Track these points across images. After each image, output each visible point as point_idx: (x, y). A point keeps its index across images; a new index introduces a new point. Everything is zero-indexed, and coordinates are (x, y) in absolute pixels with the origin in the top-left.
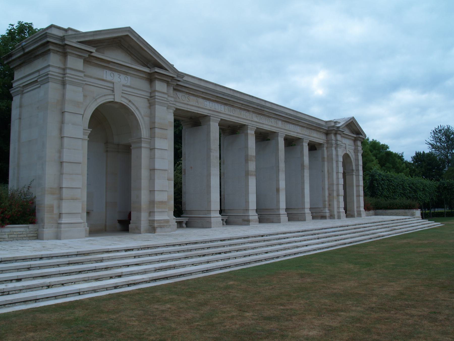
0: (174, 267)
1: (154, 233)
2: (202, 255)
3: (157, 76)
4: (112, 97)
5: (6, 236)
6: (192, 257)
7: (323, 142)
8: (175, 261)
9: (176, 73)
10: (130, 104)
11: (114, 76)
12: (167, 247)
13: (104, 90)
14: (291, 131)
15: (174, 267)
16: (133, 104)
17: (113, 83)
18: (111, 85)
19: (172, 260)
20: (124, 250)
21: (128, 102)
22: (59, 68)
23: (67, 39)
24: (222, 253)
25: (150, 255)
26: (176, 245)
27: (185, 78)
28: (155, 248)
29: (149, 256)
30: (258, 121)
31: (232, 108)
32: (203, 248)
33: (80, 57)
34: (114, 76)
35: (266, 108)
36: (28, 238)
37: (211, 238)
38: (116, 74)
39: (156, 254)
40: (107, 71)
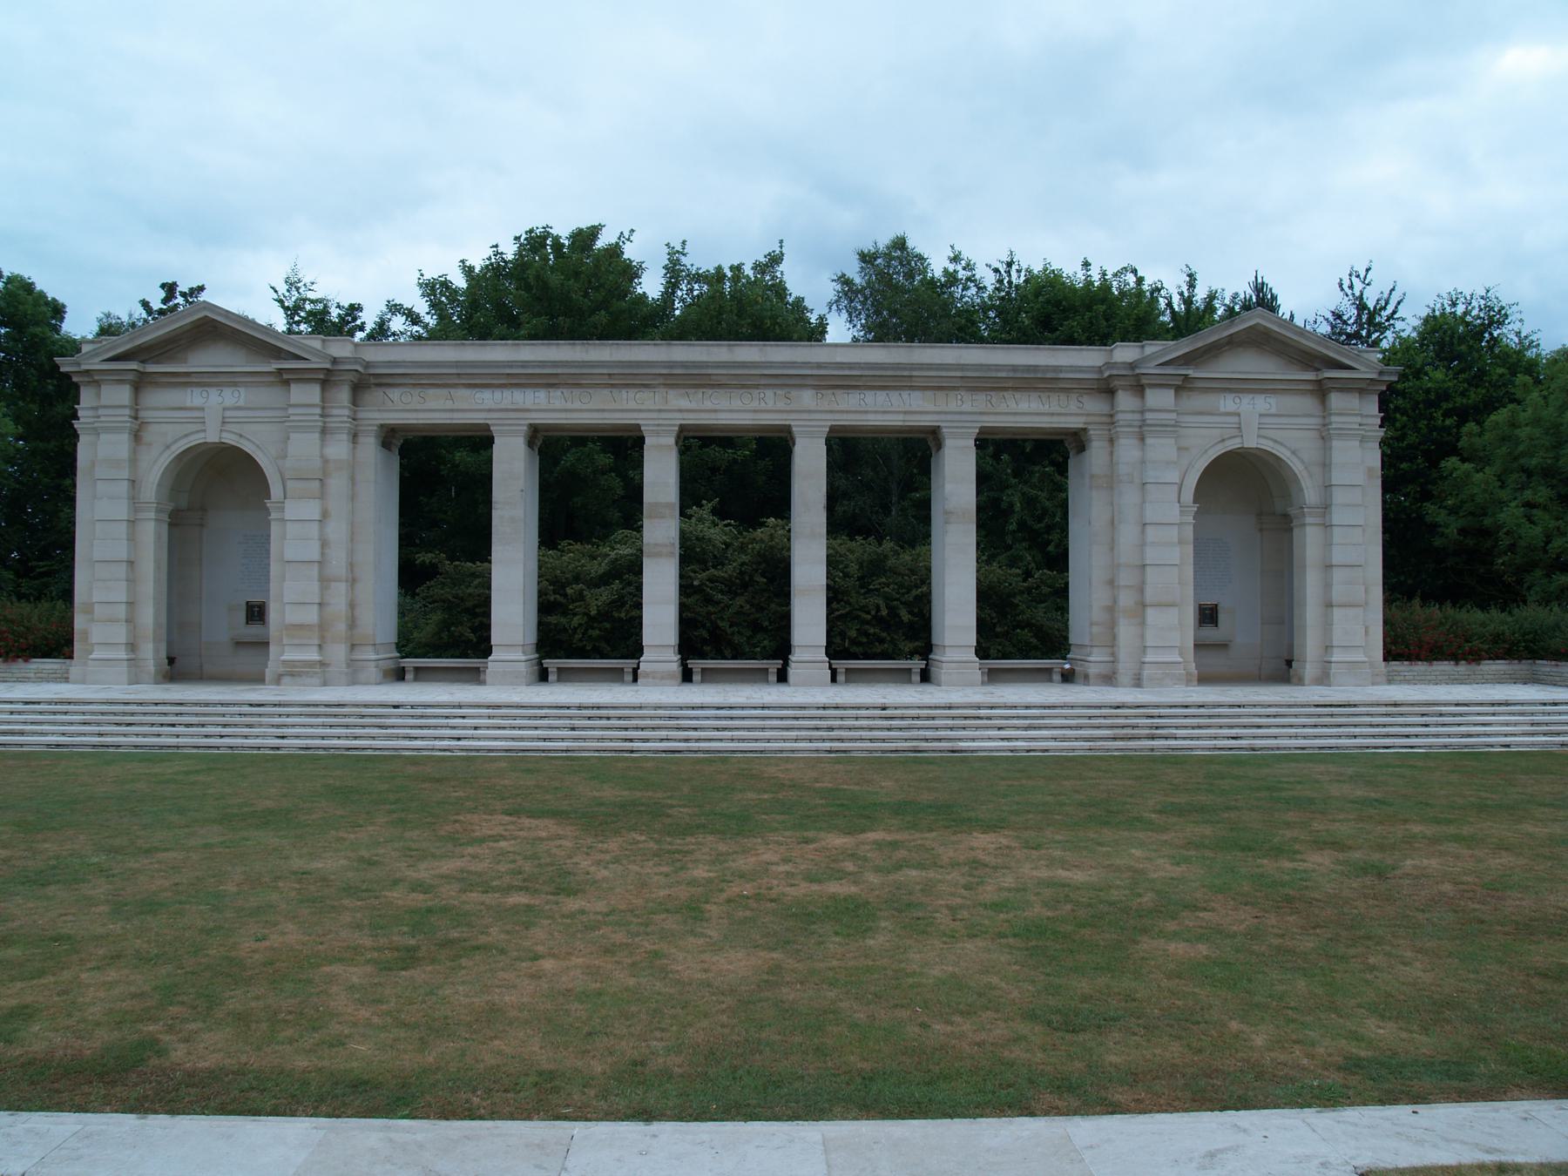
0: (22, 733)
4: (202, 435)
5: (32, 675)
7: (1085, 423)
10: (242, 441)
13: (189, 425)
14: (866, 412)
15: (22, 733)
16: (248, 440)
30: (693, 406)
31: (576, 392)
35: (708, 367)
38: (213, 392)
40: (194, 389)
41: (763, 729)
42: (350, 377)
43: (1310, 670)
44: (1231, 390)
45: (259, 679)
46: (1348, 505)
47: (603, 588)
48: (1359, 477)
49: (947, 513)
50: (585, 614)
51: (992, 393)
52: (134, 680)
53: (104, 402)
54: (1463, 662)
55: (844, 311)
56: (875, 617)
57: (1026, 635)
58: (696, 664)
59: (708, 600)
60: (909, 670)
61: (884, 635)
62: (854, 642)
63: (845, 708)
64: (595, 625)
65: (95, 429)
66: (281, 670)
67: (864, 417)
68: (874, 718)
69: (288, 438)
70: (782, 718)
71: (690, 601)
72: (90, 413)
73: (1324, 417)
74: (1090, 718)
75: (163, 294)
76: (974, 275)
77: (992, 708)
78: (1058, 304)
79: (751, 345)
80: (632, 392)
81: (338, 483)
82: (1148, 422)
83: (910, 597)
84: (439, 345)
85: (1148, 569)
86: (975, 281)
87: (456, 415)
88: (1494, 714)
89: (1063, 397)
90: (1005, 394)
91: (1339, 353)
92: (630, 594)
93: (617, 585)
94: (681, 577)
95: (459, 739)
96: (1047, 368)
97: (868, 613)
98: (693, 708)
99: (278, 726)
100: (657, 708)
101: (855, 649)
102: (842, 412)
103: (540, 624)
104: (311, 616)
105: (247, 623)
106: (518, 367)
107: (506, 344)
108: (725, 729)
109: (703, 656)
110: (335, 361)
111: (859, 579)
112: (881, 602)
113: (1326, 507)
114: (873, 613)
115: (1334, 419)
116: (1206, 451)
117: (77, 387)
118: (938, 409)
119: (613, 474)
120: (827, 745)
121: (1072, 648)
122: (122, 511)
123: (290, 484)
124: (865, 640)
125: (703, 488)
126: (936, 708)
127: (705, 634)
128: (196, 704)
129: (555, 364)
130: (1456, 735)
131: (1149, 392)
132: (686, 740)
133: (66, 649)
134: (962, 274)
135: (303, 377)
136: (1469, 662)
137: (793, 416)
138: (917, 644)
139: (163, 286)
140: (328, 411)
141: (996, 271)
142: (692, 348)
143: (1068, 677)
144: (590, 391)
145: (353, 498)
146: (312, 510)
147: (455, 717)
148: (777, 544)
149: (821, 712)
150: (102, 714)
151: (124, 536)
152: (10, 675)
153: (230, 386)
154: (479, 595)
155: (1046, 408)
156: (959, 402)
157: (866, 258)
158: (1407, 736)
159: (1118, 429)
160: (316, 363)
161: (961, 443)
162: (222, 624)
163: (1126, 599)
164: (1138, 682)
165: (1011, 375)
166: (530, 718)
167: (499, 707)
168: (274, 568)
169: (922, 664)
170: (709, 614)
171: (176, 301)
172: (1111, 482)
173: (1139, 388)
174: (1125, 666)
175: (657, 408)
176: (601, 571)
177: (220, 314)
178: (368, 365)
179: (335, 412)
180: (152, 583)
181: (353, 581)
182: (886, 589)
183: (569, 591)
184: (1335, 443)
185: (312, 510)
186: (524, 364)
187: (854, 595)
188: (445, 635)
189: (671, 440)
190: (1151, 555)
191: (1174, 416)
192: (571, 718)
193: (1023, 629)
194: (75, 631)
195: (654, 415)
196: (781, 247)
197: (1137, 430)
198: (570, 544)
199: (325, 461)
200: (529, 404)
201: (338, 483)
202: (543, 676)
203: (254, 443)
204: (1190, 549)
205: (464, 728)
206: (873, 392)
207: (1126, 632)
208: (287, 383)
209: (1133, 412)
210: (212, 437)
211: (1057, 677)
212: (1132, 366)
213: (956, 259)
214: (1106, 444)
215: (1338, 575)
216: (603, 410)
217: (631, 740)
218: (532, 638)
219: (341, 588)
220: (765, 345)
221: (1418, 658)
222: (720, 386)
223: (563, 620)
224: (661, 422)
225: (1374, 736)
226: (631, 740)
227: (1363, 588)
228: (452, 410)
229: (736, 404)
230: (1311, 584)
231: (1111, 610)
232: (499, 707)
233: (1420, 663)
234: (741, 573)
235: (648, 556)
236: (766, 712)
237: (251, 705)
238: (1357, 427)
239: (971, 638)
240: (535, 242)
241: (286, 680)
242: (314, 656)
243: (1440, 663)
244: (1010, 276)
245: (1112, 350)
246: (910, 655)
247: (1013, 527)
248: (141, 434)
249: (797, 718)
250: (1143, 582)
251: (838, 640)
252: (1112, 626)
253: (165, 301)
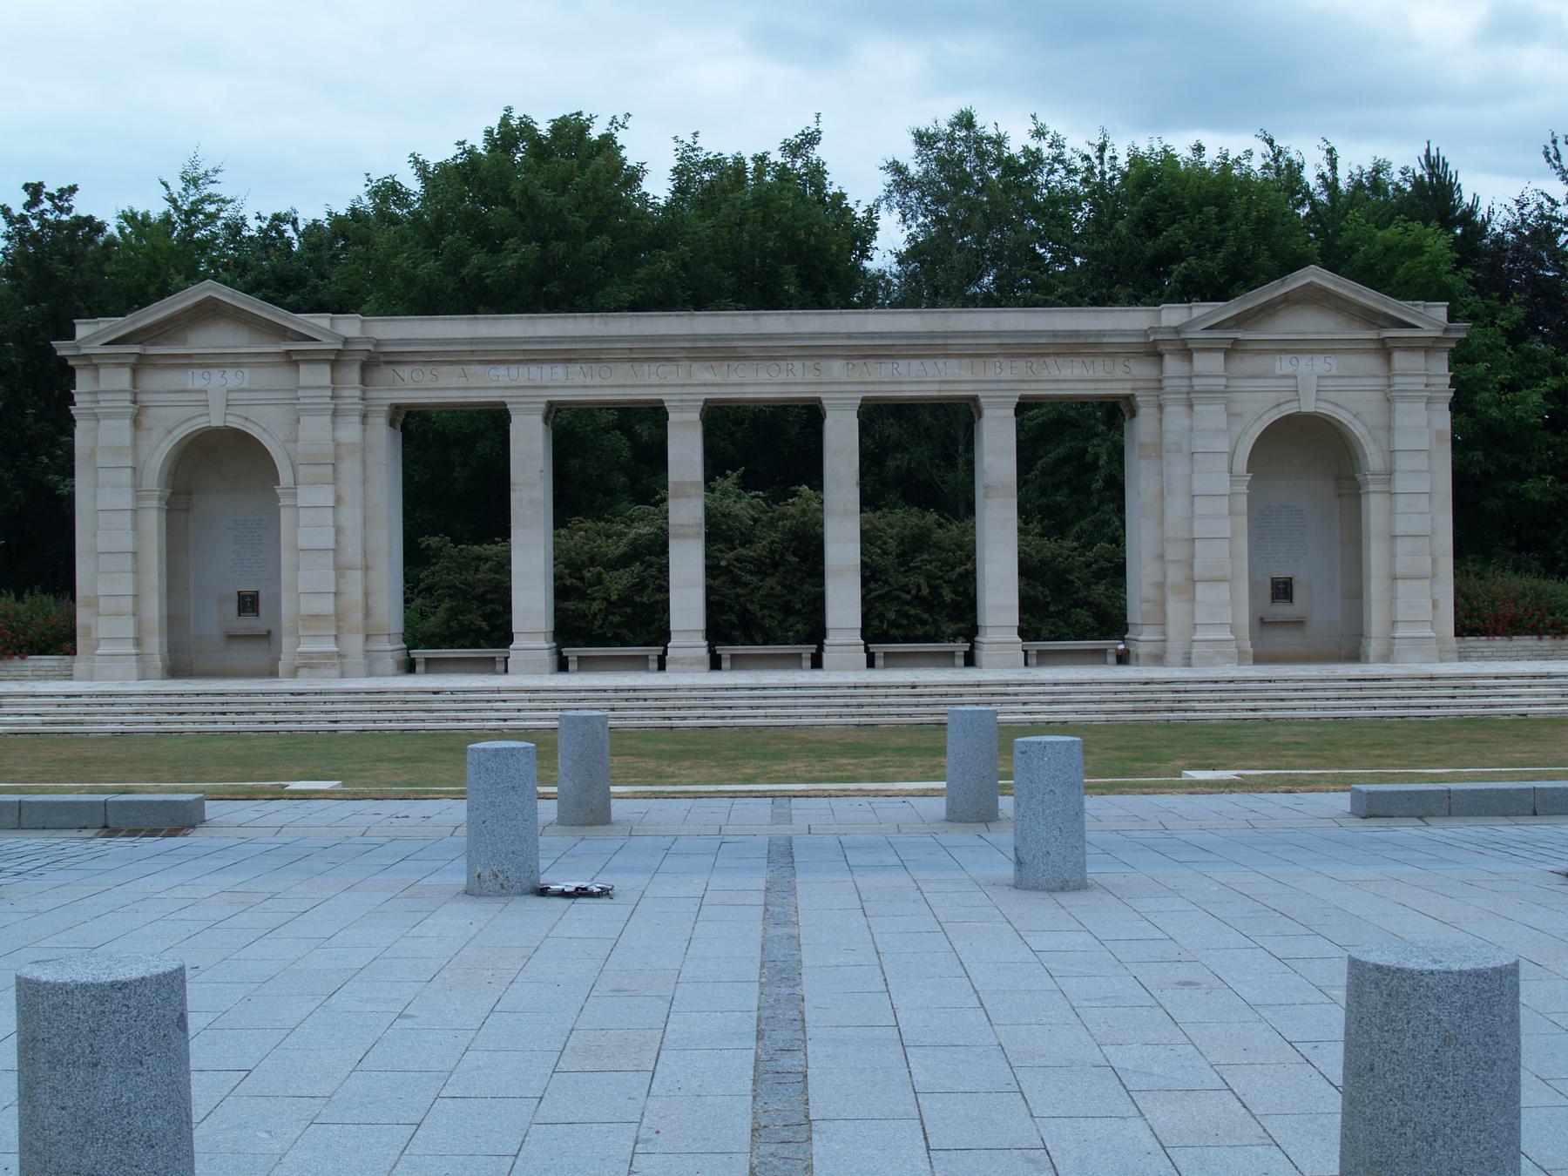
0: (82, 723)
4: (205, 419)
5: (29, 673)
7: (1132, 389)
10: (248, 424)
13: (192, 409)
14: (900, 383)
15: (82, 723)
16: (256, 424)
30: (718, 379)
31: (596, 367)
35: (733, 340)
38: (216, 373)
40: (195, 371)
41: (795, 707)
42: (363, 357)
43: (1374, 647)
44: (1287, 352)
45: (273, 673)
46: (1413, 472)
47: (621, 570)
48: (1423, 442)
49: (985, 487)
50: (604, 599)
51: (1033, 360)
52: (143, 677)
53: (102, 387)
54: (1547, 637)
55: (897, 210)
56: (917, 597)
57: (1083, 615)
58: (725, 651)
59: (737, 582)
60: (953, 653)
61: (926, 616)
62: (893, 624)
63: (875, 687)
64: (615, 610)
65: (96, 415)
66: (298, 662)
67: (898, 388)
68: (903, 696)
69: (298, 421)
70: (813, 697)
71: (718, 582)
72: (87, 398)
73: (1389, 377)
74: (1116, 693)
75: (26, 197)
76: (1062, 154)
77: (1020, 685)
78: (1163, 198)
79: (778, 314)
80: (654, 366)
81: (350, 468)
82: (1196, 388)
83: (953, 575)
84: (450, 319)
85: (1197, 543)
86: (1062, 162)
87: (470, 393)
88: (1529, 686)
89: (1108, 362)
90: (1047, 360)
91: (1400, 311)
92: (652, 576)
93: (637, 567)
94: (707, 557)
95: (505, 720)
96: (1089, 333)
97: (908, 592)
98: (727, 689)
99: (327, 712)
100: (691, 689)
101: (894, 632)
102: (874, 383)
103: (556, 610)
104: (326, 606)
105: (239, 615)
106: (534, 342)
107: (521, 318)
108: (758, 707)
109: (732, 642)
110: (346, 341)
111: (898, 556)
112: (922, 582)
113: (1389, 474)
114: (914, 592)
115: (1396, 380)
116: (1260, 417)
117: (71, 372)
118: (976, 378)
119: (618, 433)
120: (856, 720)
121: (1130, 627)
122: (126, 500)
123: (302, 470)
124: (905, 622)
125: (722, 444)
126: (965, 685)
127: (734, 618)
129: (574, 339)
130: (1478, 706)
131: (1196, 356)
132: (722, 718)
133: (68, 646)
134: (1047, 152)
135: (313, 358)
136: (1554, 636)
137: (822, 388)
138: (961, 625)
139: (26, 187)
140: (338, 393)
141: (1087, 158)
142: (716, 319)
143: (1123, 659)
144: (610, 365)
145: (365, 481)
146: (325, 496)
147: (497, 701)
148: (811, 519)
149: (852, 691)
150: (149, 704)
151: (130, 527)
152: (5, 673)
153: (231, 367)
154: (489, 581)
155: (1090, 374)
156: (998, 370)
157: (924, 140)
158: (1428, 707)
159: (1165, 396)
160: (328, 344)
161: (1002, 413)
162: (216, 616)
163: (1175, 575)
164: (1188, 662)
165: (1052, 340)
166: (569, 700)
167: (537, 691)
168: (286, 557)
169: (966, 646)
170: (738, 596)
171: (42, 207)
172: (1159, 451)
173: (1186, 352)
174: (1175, 646)
175: (681, 382)
176: (618, 552)
178: (378, 343)
179: (346, 393)
180: (156, 576)
181: (367, 569)
182: (928, 567)
183: (587, 575)
184: (1399, 406)
185: (325, 496)
186: (542, 340)
187: (892, 572)
188: (454, 624)
189: (695, 416)
190: (1199, 529)
191: (1223, 381)
192: (609, 700)
193: (1081, 607)
194: (78, 626)
195: (678, 390)
196: (818, 122)
197: (1184, 396)
198: (581, 522)
199: (337, 445)
200: (546, 381)
201: (350, 468)
202: (562, 666)
203: (260, 426)
204: (1243, 521)
205: (508, 710)
206: (906, 361)
207: (1174, 608)
208: (296, 363)
209: (1181, 377)
210: (217, 422)
211: (1112, 659)
212: (1177, 330)
213: (1039, 133)
214: (1155, 410)
215: (1402, 546)
216: (625, 386)
217: (670, 718)
218: (551, 627)
219: (357, 575)
220: (792, 314)
221: (1495, 633)
222: (747, 358)
223: (583, 606)
224: (686, 397)
225: (1394, 707)
226: (670, 718)
227: (1429, 560)
228: (466, 389)
229: (763, 376)
230: (1375, 555)
231: (1161, 586)
232: (537, 691)
233: (1497, 638)
234: (772, 551)
235: (675, 537)
236: (798, 692)
237: (292, 694)
238: (1423, 387)
239: (1014, 619)
240: (509, 135)
241: (303, 672)
242: (331, 647)
243: (1520, 638)
244: (1102, 163)
245: (1160, 311)
246: (953, 638)
247: (1098, 485)
249: (828, 697)
250: (1193, 557)
251: (876, 622)
252: (1162, 603)
253: (28, 206)
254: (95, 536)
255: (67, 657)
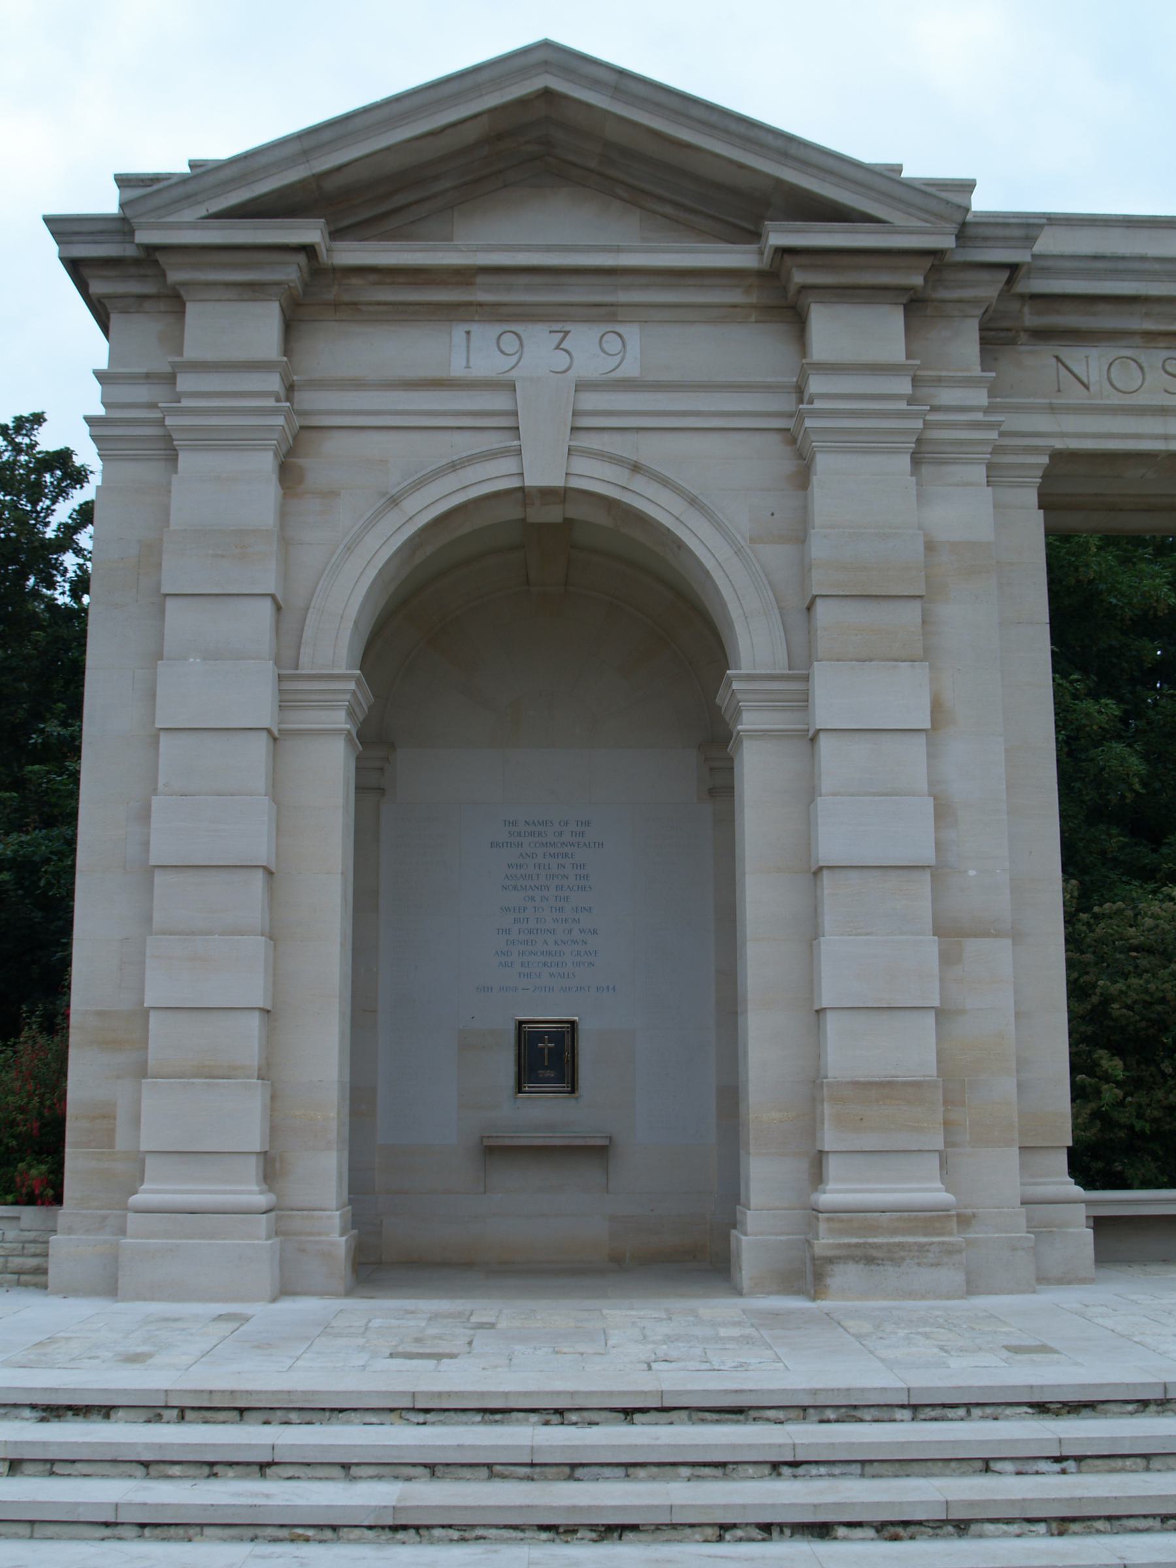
1: (814, 1299)
2: (592, 1528)
3: (800, 277)
4: (507, 465)
6: (473, 1527)
8: (275, 1540)
9: (940, 217)
10: (639, 483)
11: (522, 345)
12: (421, 1418)
13: (458, 438)
16: (665, 482)
17: (511, 387)
18: (499, 401)
19: (250, 1532)
20: (33, 1407)
21: (627, 472)
22: (148, 377)
23: (136, 220)
24: (841, 1531)
25: (153, 1470)
26: (514, 1414)
27: (1047, 243)
28: (308, 1416)
29: (140, 1471)
32: (723, 1465)
33: (254, 290)
34: (522, 345)
36: (15, 1277)
37: (913, 1384)
39: (211, 1468)
40: (475, 328)
53: (191, 352)
128: (802, 1411)
177: (595, 84)
179: (947, 396)
237: (1042, 1408)
248: (300, 461)
254: (144, 815)
255: (29, 1214)
